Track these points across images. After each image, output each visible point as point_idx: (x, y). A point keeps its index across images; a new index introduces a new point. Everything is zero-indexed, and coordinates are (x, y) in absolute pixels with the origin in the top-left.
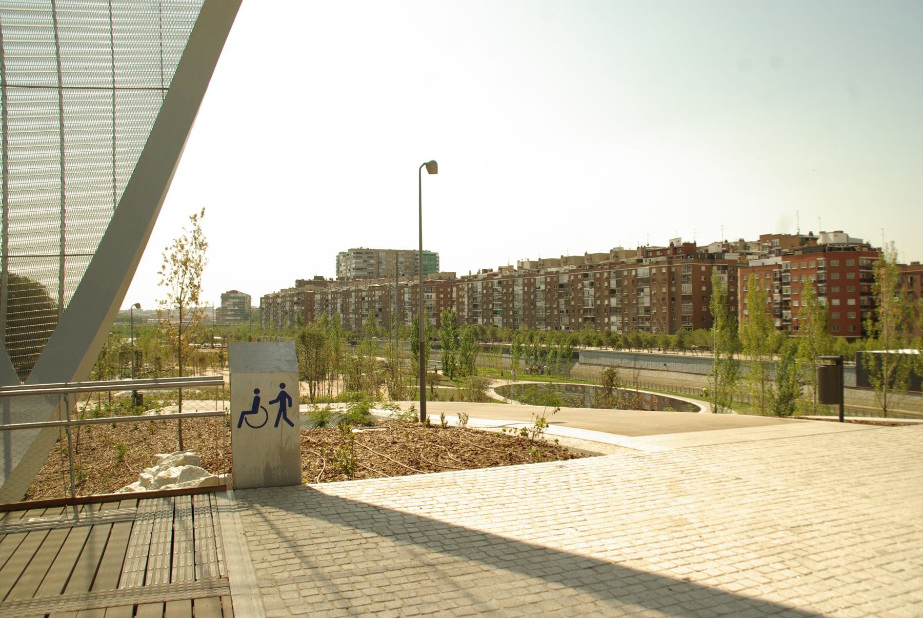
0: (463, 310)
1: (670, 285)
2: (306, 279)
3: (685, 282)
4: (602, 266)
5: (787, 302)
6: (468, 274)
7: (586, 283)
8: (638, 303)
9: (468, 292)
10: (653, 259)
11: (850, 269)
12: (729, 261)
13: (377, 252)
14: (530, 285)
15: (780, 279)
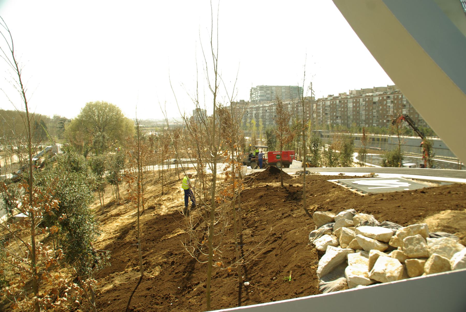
0: (320, 116)
6: (322, 97)
7: (389, 101)
9: (322, 107)
13: (271, 87)
14: (356, 103)
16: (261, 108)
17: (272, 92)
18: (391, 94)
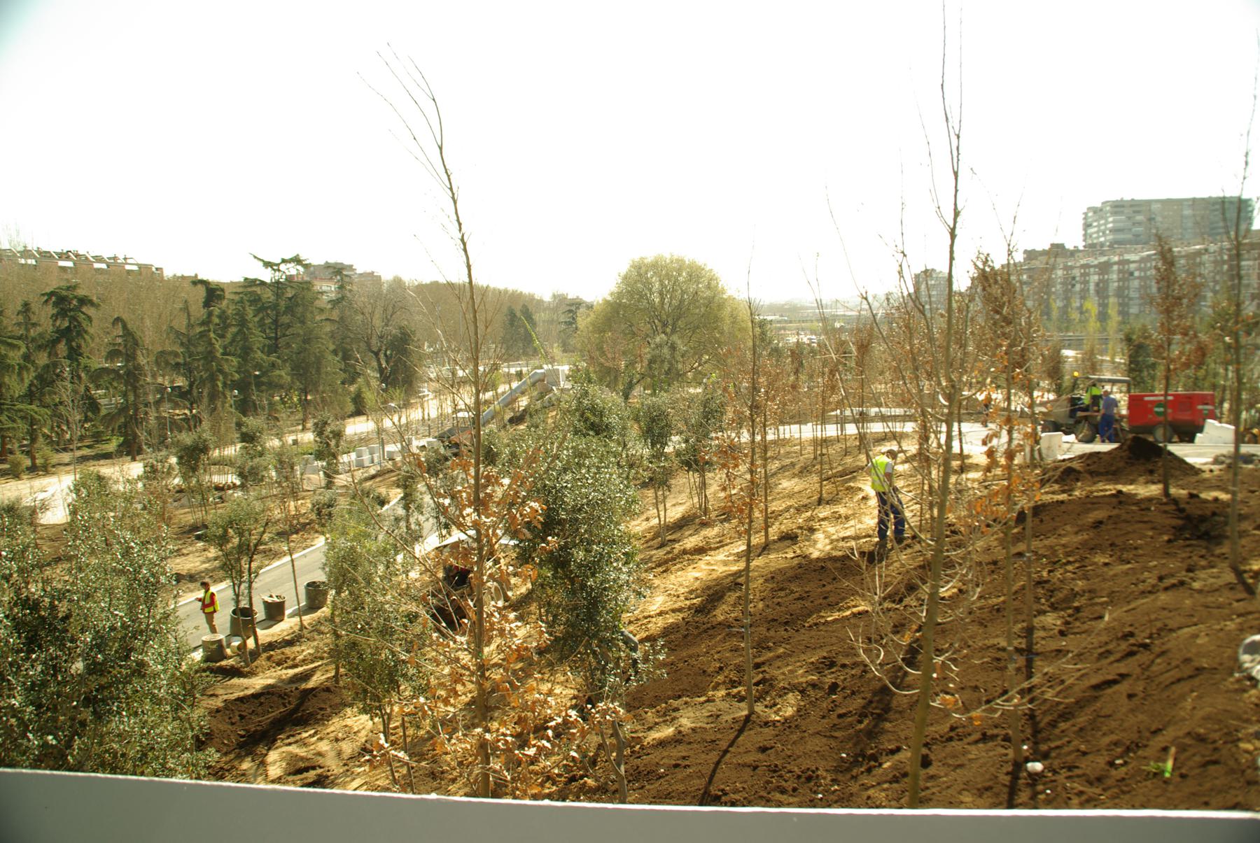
2: (1039, 248)
16: (1115, 267)
17: (1151, 220)
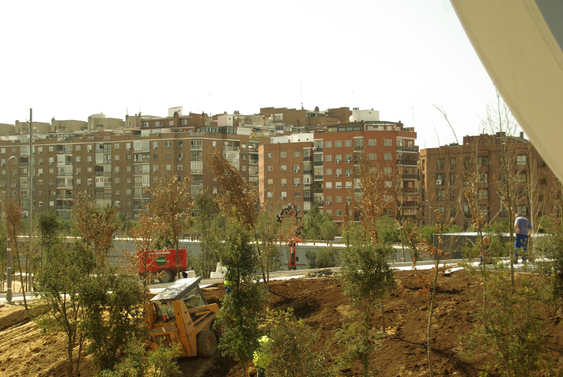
1: (177, 162)
3: (195, 160)
4: (86, 138)
5: (319, 184)
7: (62, 158)
8: (133, 183)
10: (154, 131)
11: (388, 149)
12: (242, 136)
15: (311, 159)
18: (68, 140)
